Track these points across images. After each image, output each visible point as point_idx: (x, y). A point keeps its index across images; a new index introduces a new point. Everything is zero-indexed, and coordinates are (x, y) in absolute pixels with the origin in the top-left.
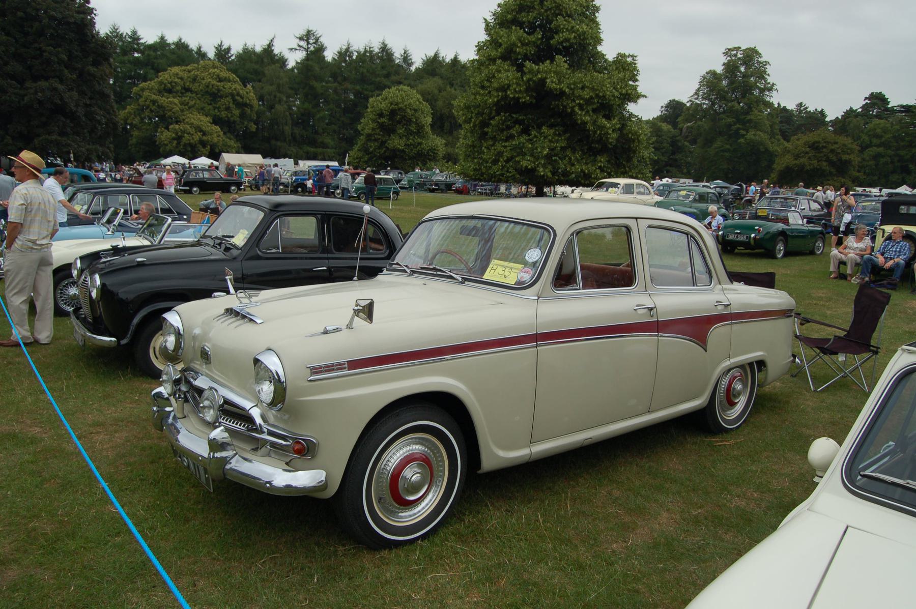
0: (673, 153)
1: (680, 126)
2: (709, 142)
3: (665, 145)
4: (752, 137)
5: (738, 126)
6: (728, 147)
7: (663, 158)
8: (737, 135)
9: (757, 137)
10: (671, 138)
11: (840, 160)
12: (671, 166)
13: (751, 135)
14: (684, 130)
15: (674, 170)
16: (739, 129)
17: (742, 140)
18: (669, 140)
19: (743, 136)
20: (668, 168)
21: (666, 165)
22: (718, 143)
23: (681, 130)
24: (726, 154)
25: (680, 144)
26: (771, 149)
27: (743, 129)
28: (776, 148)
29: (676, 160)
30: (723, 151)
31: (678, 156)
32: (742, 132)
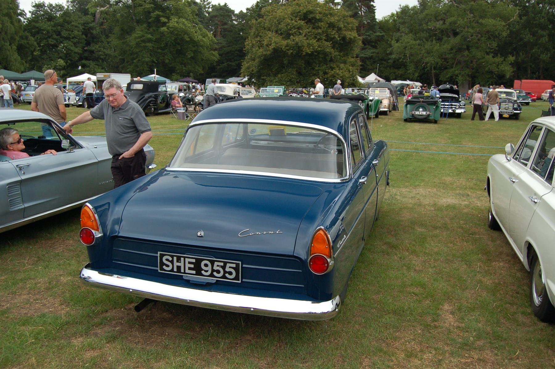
0: (88, 44)
1: (92, 10)
2: (126, 32)
3: (76, 32)
4: (176, 24)
5: (157, 12)
6: (149, 36)
7: (76, 50)
8: (158, 22)
9: (181, 25)
10: (84, 24)
11: (344, 39)
12: (87, 59)
13: (174, 22)
14: (98, 16)
15: (92, 64)
16: (158, 17)
17: (165, 29)
18: (81, 27)
19: (164, 24)
20: (84, 62)
21: (81, 59)
22: (139, 32)
23: (94, 15)
24: (149, 45)
25: (94, 32)
26: (196, 39)
27: (163, 17)
28: (200, 37)
29: (92, 52)
30: (143, 41)
31: (94, 47)
32: (163, 20)
